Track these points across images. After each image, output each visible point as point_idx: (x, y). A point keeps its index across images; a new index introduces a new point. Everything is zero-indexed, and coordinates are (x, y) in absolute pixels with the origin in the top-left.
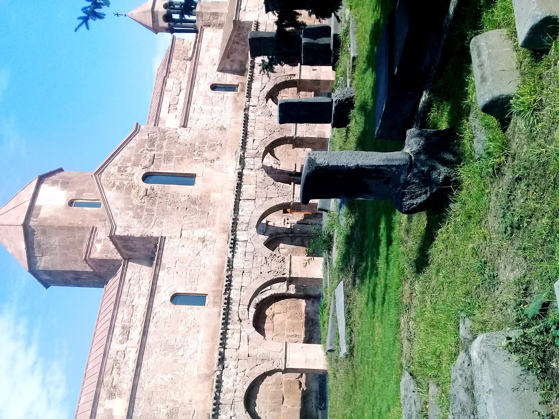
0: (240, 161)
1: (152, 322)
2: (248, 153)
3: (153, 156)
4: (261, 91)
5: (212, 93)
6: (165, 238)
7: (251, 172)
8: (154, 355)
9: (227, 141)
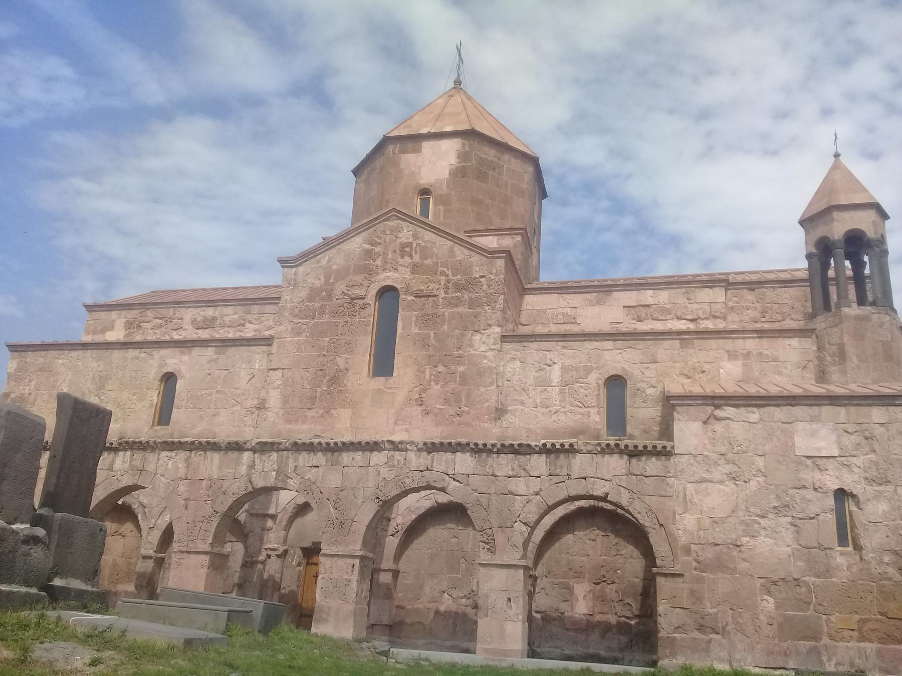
0: (265, 443)
1: (140, 353)
2: (288, 457)
3: (431, 294)
4: (448, 475)
5: (595, 379)
6: (270, 345)
7: (245, 467)
8: (95, 364)
9: (468, 425)
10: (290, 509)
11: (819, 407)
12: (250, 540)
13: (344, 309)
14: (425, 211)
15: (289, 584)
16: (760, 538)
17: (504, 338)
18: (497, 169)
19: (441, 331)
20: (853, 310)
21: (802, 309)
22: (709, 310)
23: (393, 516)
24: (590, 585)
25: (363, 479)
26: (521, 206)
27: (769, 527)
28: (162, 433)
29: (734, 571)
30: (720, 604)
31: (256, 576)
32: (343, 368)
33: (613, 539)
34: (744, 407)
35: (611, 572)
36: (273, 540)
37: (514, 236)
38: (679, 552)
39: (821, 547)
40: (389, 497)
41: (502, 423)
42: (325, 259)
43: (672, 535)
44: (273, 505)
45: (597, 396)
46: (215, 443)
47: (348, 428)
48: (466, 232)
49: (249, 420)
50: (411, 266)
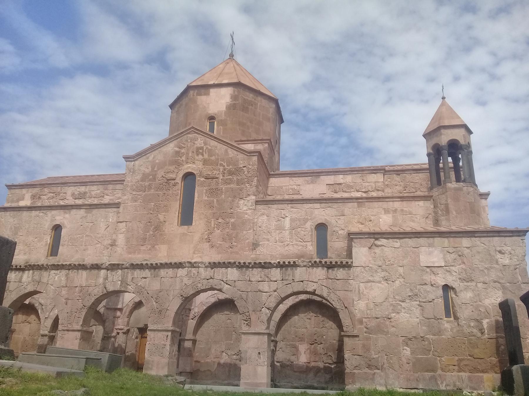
0: (114, 265)
1: (39, 213)
2: (128, 273)
3: (214, 177)
4: (223, 281)
5: (310, 225)
6: (119, 208)
8: (11, 220)
9: (237, 253)
10: (131, 305)
11: (433, 238)
12: (107, 324)
13: (163, 186)
14: (212, 129)
15: (130, 350)
16: (402, 313)
17: (257, 202)
18: (254, 105)
19: (221, 198)
20: (453, 184)
21: (426, 185)
22: (375, 186)
23: (192, 308)
24: (308, 346)
25: (173, 285)
26: (268, 127)
27: (407, 307)
28: (53, 260)
29: (388, 332)
30: (380, 352)
31: (110, 345)
32: (162, 221)
33: (321, 318)
34: (392, 239)
35: (320, 337)
36: (121, 323)
37: (264, 144)
38: (356, 323)
39: (435, 318)
40: (188, 295)
41: (256, 252)
42: (151, 157)
43: (352, 313)
44: (120, 303)
45: (311, 235)
46: (83, 265)
47: (165, 256)
48: (236, 141)
49: (106, 252)
50: (203, 161)
